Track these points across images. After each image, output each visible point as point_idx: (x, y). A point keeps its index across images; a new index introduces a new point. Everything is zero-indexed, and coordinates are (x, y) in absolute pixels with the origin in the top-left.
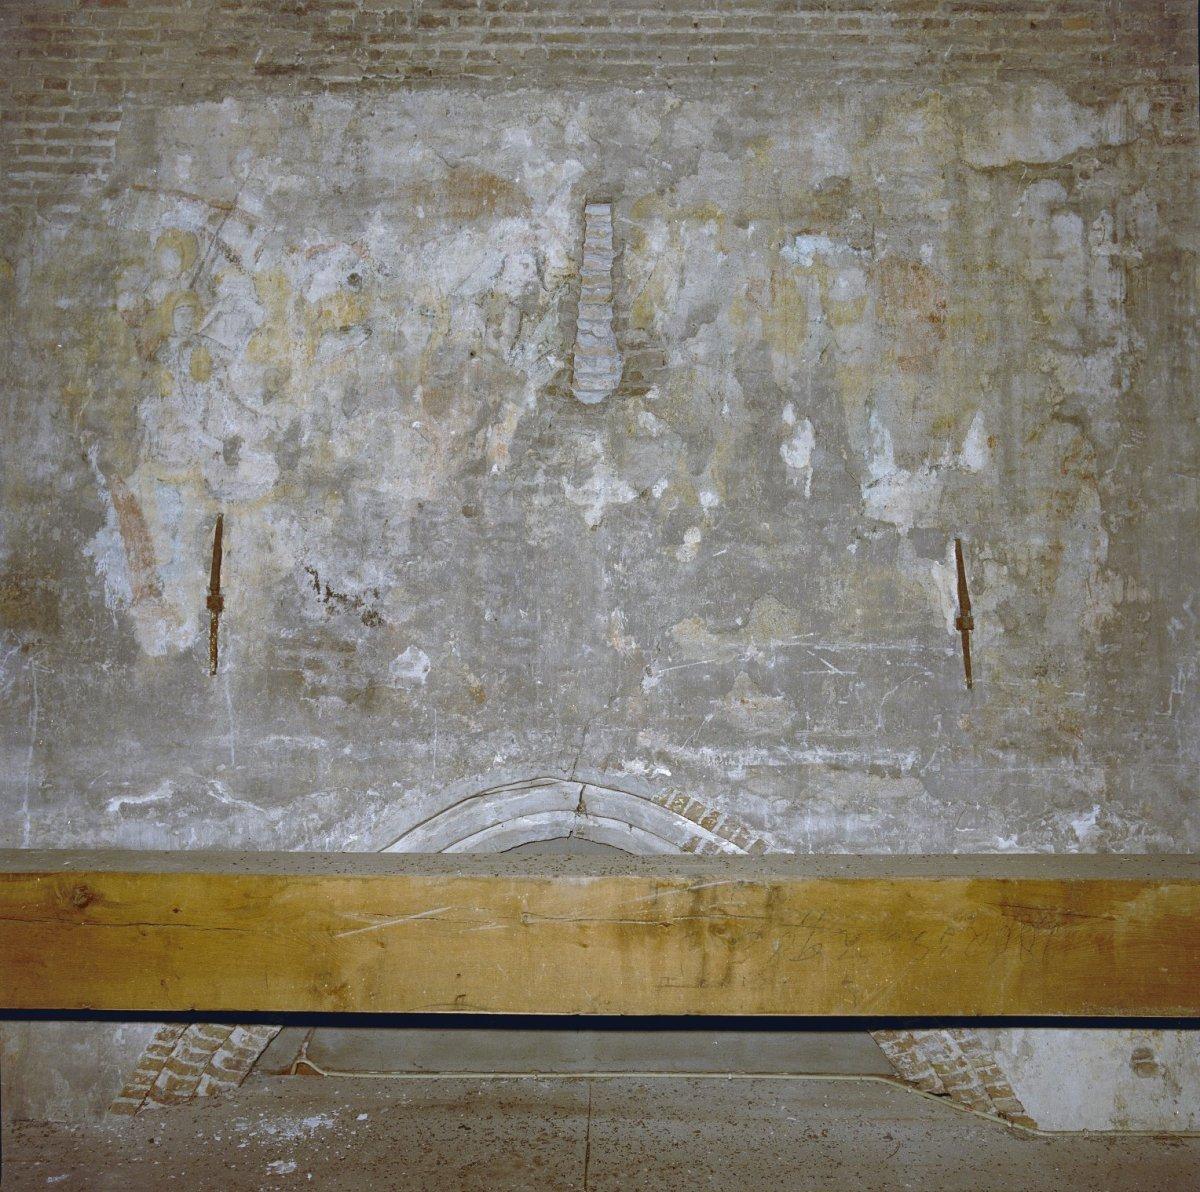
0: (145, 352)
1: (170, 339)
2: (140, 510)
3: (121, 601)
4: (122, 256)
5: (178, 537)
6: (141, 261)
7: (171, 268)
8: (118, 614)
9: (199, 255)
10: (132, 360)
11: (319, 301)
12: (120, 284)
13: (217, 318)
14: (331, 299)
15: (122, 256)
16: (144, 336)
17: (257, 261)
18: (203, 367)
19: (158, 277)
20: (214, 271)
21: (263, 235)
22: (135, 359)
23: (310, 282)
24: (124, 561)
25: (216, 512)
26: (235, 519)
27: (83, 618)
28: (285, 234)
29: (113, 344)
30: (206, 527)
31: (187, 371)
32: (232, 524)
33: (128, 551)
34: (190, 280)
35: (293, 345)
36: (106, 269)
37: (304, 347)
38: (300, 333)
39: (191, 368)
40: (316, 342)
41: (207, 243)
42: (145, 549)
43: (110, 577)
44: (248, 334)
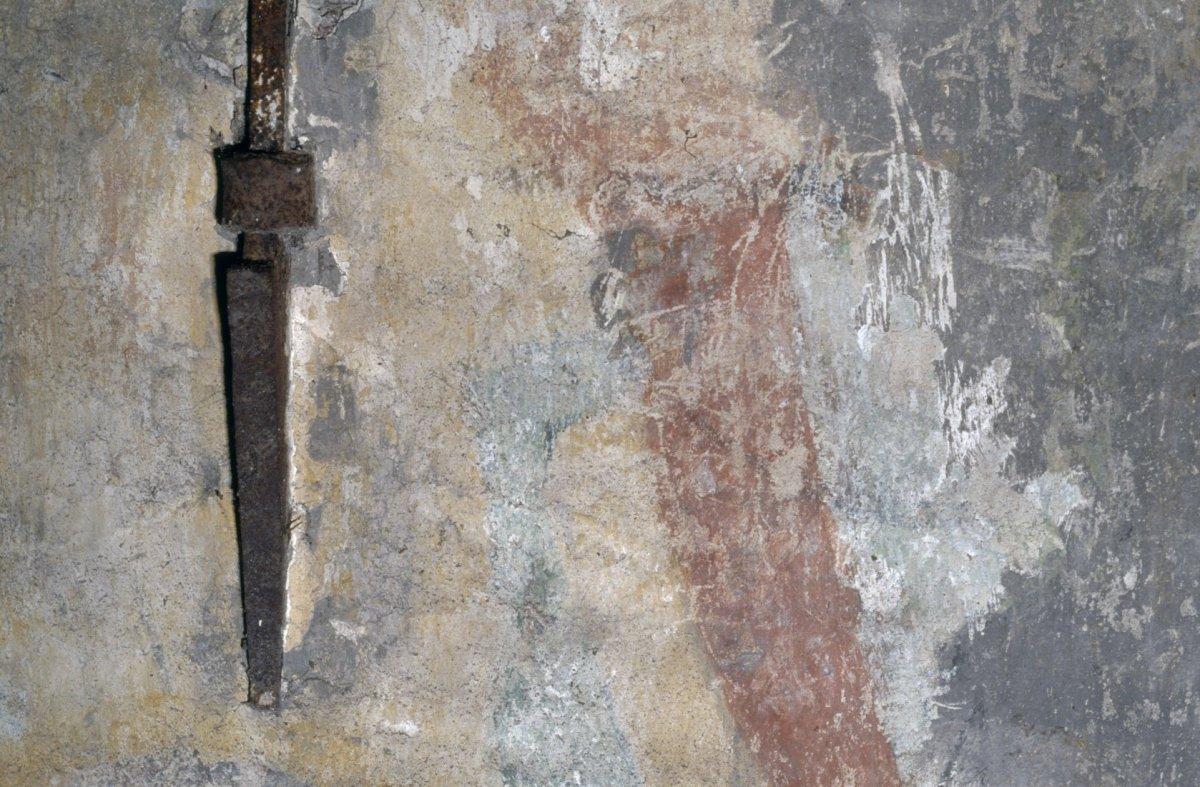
2: (741, 734)
3: (855, 205)
5: (514, 574)
8: (873, 127)
24: (834, 441)
25: (291, 717)
26: (183, 679)
27: (1091, 104)
30: (341, 628)
32: (202, 647)
33: (811, 500)
42: (714, 511)
43: (919, 349)
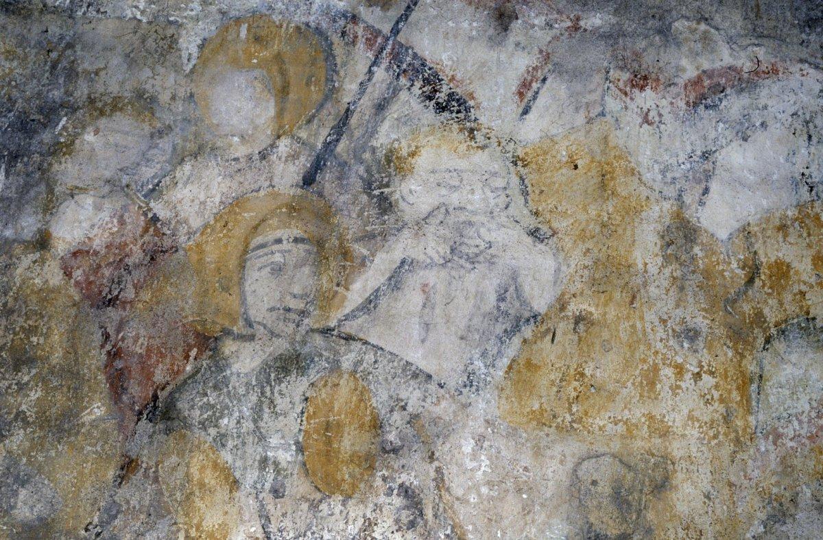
0: (136, 390)
1: (229, 347)
4: (82, 90)
6: (144, 103)
7: (244, 126)
9: (334, 90)
10: (87, 418)
11: (746, 232)
12: (67, 171)
13: (395, 281)
14: (783, 228)
15: (82, 90)
16: (137, 339)
17: (526, 112)
18: (350, 442)
19: (200, 151)
20: (385, 136)
21: (544, 37)
22: (97, 410)
23: (708, 176)
28: (611, 37)
29: (21, 359)
31: (286, 457)
34: (304, 162)
35: (668, 372)
36: (25, 126)
37: (708, 380)
38: (691, 335)
39: (301, 449)
40: (752, 368)
41: (362, 56)
44: (509, 333)
